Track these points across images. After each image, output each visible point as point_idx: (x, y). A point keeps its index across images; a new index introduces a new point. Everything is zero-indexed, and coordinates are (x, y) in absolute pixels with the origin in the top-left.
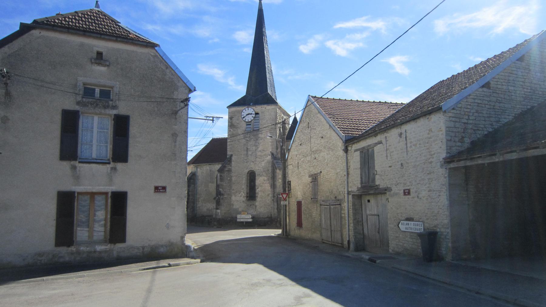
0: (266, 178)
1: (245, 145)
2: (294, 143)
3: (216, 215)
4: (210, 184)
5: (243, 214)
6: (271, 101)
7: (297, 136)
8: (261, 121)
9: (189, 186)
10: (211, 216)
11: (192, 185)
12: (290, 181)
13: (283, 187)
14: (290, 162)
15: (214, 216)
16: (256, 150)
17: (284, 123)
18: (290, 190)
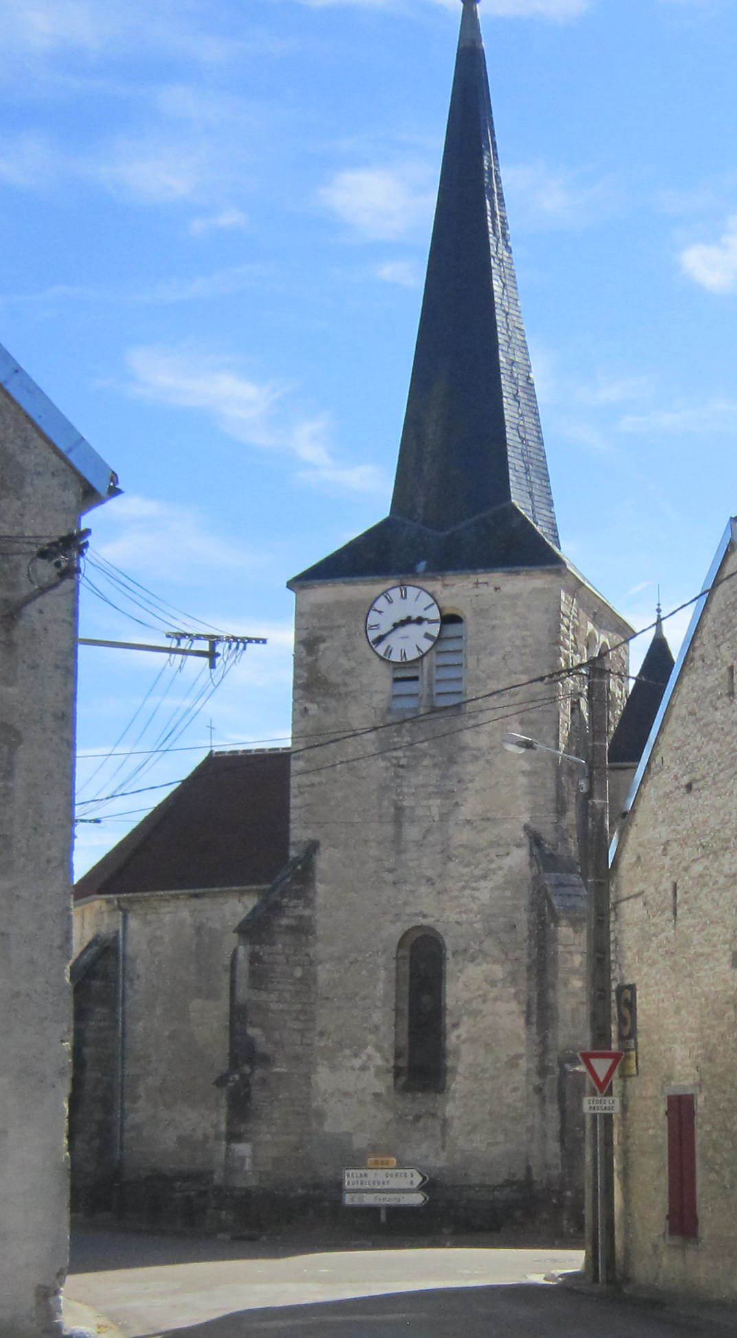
0: (499, 971)
1: (384, 788)
2: (654, 779)
3: (229, 1170)
4: (196, 1003)
5: (377, 1166)
6: (528, 550)
7: (667, 739)
8: (471, 661)
9: (80, 1014)
10: (199, 1176)
11: (100, 1011)
12: (632, 988)
13: (594, 1017)
14: (628, 880)
15: (218, 1178)
16: (444, 817)
17: (597, 669)
18: (629, 1034)
